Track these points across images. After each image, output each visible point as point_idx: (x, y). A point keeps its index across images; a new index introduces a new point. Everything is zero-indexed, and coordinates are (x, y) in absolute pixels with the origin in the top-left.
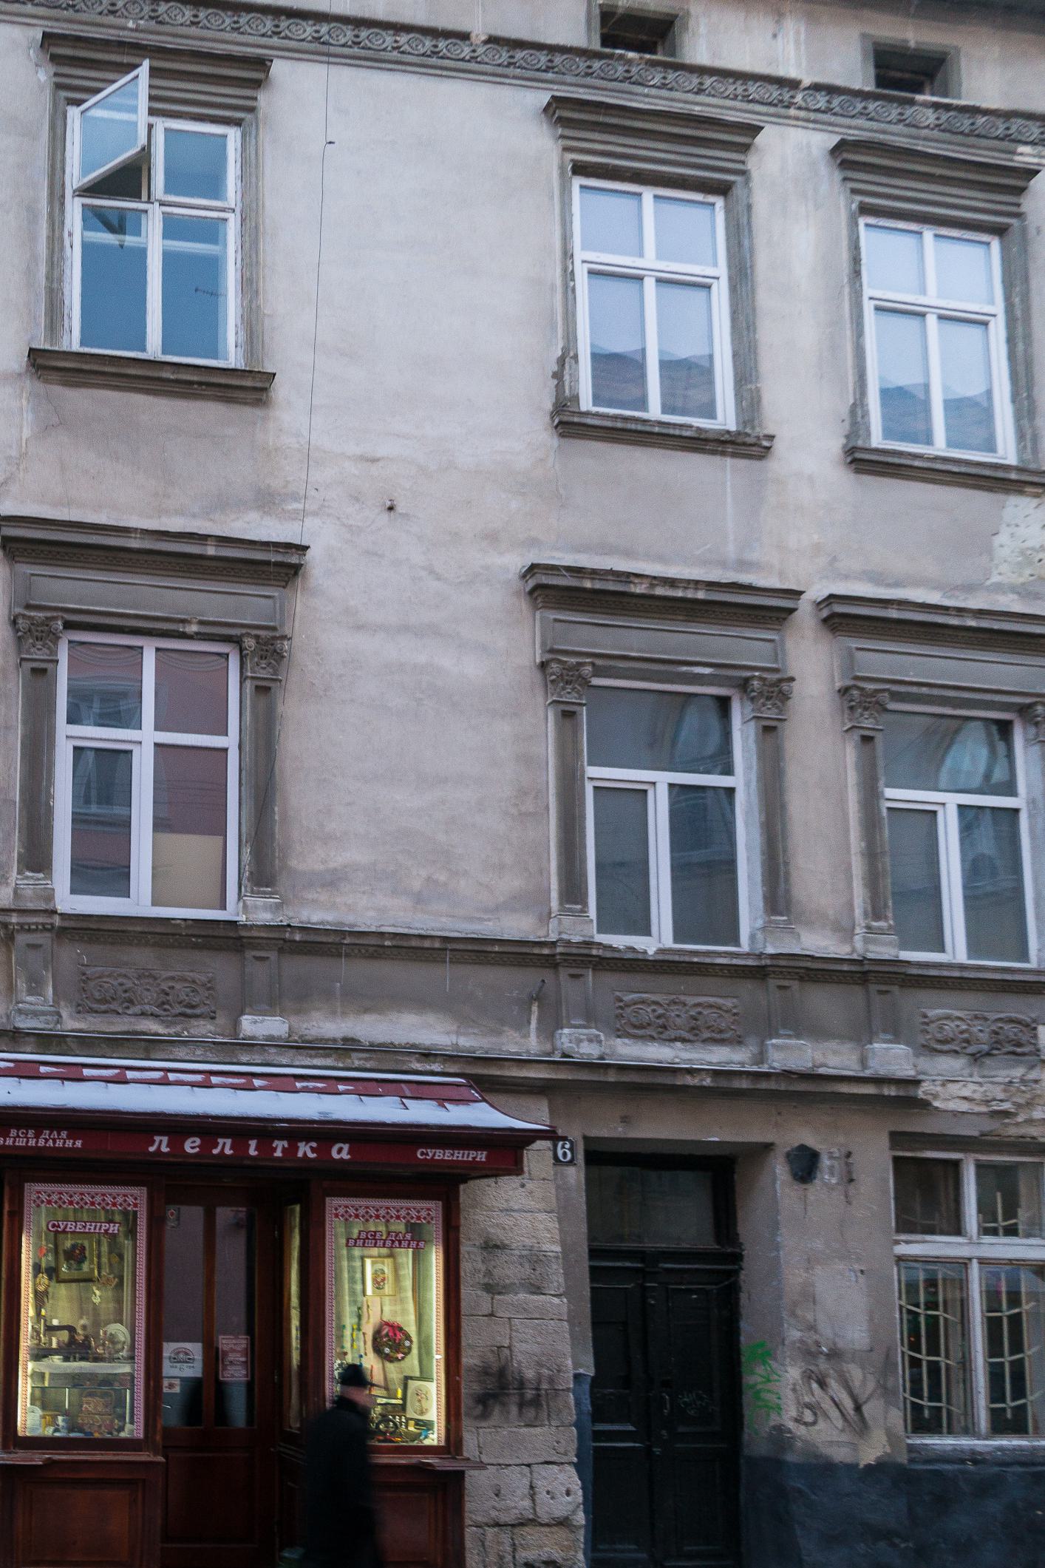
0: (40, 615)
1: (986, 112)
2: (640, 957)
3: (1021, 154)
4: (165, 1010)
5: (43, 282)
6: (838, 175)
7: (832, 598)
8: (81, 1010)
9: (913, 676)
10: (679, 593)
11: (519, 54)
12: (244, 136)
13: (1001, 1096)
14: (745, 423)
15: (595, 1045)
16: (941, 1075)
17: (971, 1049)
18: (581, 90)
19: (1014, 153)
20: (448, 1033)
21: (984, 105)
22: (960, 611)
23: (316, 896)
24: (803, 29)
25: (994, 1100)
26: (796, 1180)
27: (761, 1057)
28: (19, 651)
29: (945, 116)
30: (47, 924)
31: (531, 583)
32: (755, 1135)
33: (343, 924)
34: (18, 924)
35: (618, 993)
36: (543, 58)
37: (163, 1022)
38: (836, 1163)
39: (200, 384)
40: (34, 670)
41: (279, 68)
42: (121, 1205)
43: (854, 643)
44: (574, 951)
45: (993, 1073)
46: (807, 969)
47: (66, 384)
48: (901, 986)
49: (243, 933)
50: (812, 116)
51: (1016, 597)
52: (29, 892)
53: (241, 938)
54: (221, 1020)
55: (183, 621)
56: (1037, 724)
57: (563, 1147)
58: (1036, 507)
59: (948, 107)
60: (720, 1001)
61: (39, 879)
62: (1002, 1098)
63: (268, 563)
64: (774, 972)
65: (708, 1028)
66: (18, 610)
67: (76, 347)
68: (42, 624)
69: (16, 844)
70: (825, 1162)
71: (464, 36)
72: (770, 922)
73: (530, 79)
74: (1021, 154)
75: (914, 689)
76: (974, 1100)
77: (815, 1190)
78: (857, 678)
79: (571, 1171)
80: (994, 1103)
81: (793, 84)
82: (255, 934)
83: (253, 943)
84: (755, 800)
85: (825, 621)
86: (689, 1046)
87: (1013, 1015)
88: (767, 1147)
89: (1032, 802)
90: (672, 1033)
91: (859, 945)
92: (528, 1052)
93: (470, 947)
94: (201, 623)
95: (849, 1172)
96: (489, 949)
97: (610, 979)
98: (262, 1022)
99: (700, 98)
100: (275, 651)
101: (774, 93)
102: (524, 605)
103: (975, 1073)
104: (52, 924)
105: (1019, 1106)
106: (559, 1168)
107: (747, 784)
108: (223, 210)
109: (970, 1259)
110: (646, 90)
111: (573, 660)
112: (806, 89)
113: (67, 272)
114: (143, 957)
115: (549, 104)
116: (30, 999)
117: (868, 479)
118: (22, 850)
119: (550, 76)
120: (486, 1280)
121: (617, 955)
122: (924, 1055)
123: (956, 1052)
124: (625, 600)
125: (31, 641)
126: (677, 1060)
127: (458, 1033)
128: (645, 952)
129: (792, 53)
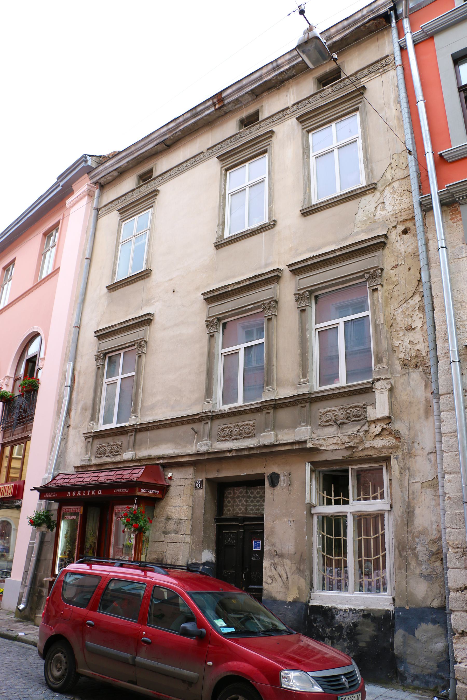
2: (223, 412)
3: (363, 81)
9: (320, 281)
13: (348, 440)
15: (206, 446)
16: (326, 436)
19: (361, 82)
20: (173, 449)
25: (345, 442)
32: (258, 471)
33: (154, 420)
35: (219, 427)
41: (158, 189)
44: (204, 415)
45: (347, 431)
49: (126, 429)
51: (364, 234)
55: (126, 344)
57: (198, 483)
62: (348, 441)
64: (264, 408)
65: (245, 433)
70: (282, 478)
74: (363, 81)
75: (321, 286)
76: (339, 444)
79: (201, 491)
80: (345, 444)
86: (238, 441)
90: (233, 438)
103: (339, 433)
105: (357, 443)
106: (197, 490)
109: (348, 512)
114: (109, 440)
120: (164, 530)
121: (217, 413)
122: (319, 429)
124: (228, 293)
126: (234, 447)
127: (175, 449)
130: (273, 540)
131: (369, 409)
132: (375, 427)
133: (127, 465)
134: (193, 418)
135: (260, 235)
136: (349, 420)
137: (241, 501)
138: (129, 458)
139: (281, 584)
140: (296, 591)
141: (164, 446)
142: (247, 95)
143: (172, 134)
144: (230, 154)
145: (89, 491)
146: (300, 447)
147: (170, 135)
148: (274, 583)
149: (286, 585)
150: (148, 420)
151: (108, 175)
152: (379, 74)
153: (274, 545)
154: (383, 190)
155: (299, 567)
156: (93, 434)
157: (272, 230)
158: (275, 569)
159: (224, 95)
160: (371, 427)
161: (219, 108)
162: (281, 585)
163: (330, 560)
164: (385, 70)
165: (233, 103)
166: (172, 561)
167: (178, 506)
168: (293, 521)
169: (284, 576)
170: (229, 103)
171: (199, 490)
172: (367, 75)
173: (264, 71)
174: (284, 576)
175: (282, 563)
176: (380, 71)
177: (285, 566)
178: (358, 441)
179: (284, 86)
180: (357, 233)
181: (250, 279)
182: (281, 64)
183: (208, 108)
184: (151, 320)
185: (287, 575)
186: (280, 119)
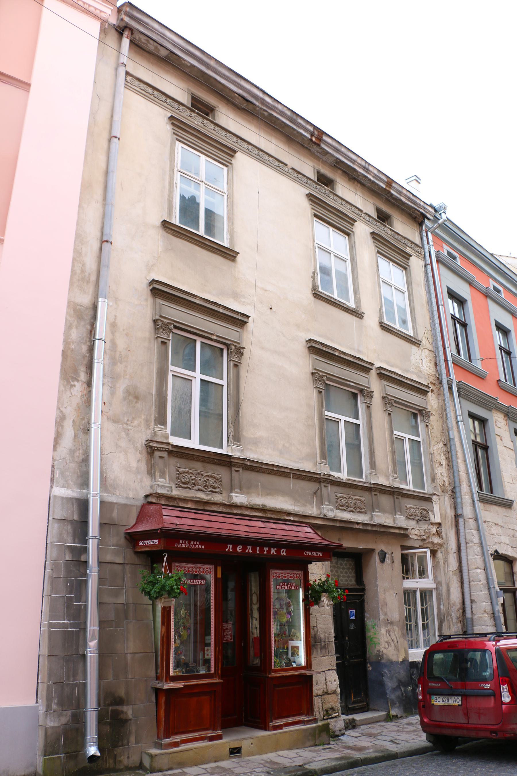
0: (166, 321)
1: (400, 235)
4: (206, 489)
5: (167, 197)
6: (372, 240)
7: (380, 368)
8: (178, 486)
10: (346, 358)
11: (300, 176)
12: (228, 171)
14: (357, 307)
15: (332, 512)
17: (417, 518)
21: (400, 233)
22: (407, 378)
23: (251, 447)
27: (372, 518)
28: (155, 333)
29: (393, 233)
31: (309, 345)
32: (370, 546)
33: (259, 459)
34: (156, 447)
35: (336, 493)
36: (305, 180)
37: (205, 494)
40: (162, 342)
42: (191, 571)
43: (386, 383)
46: (381, 489)
48: (401, 497)
49: (232, 460)
50: (366, 221)
52: (159, 433)
53: (231, 462)
54: (224, 495)
55: (212, 334)
56: (423, 416)
59: (393, 231)
60: (361, 498)
61: (162, 429)
63: (238, 319)
65: (358, 507)
66: (157, 317)
67: (177, 223)
68: (166, 325)
69: (153, 412)
71: (286, 165)
72: (371, 472)
78: (386, 394)
81: (362, 211)
82: (236, 461)
83: (236, 465)
84: (366, 430)
85: (378, 374)
87: (424, 508)
88: (373, 550)
89: (423, 440)
90: (350, 509)
91: (391, 482)
92: (314, 513)
93: (297, 473)
94: (217, 336)
95: (393, 559)
96: (303, 474)
97: (335, 489)
98: (239, 496)
99: (341, 206)
100: (240, 352)
101: (358, 212)
102: (306, 351)
104: (168, 449)
107: (363, 424)
108: (223, 193)
110: (330, 199)
111: (321, 374)
113: (174, 196)
114: (198, 466)
115: (308, 194)
116: (160, 480)
117: (384, 331)
118: (157, 416)
119: (307, 185)
123: (413, 519)
124: (333, 356)
125: (161, 330)
128: (343, 480)
131: (430, 513)
133: (247, 513)
134: (313, 476)
138: (242, 503)
139: (394, 647)
141: (280, 498)
144: (321, 203)
145: (266, 549)
146: (404, 533)
147: (260, 106)
149: (397, 649)
150: (251, 456)
151: (155, 44)
153: (386, 614)
156: (170, 448)
159: (324, 138)
161: (314, 143)
164: (418, 256)
169: (396, 641)
176: (417, 253)
178: (427, 536)
179: (354, 183)
180: (412, 373)
181: (354, 357)
182: (370, 171)
183: (306, 130)
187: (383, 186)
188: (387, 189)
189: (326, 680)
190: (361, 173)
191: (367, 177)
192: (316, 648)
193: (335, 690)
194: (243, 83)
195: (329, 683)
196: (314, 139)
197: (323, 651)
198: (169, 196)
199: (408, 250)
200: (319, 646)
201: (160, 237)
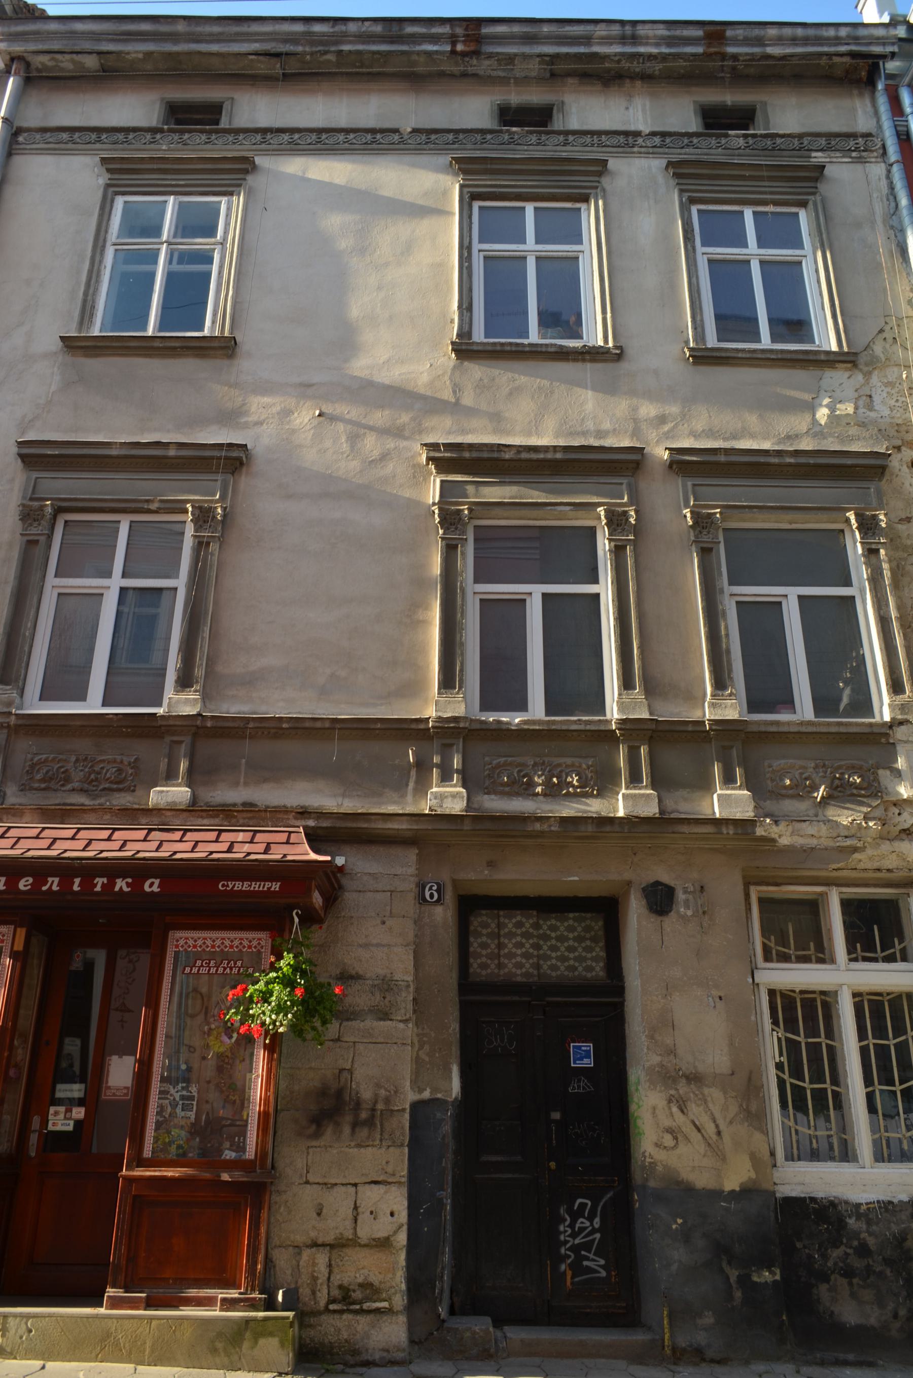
3: (815, 157)
6: (673, 182)
18: (478, 152)
19: (810, 157)
20: (335, 796)
24: (648, 103)
26: (653, 912)
30: (5, 723)
35: (487, 759)
38: (691, 897)
39: (182, 348)
47: (86, 356)
55: (147, 501)
57: (431, 888)
58: (849, 378)
61: (7, 690)
70: (681, 896)
71: (396, 131)
73: (441, 150)
74: (815, 157)
77: (670, 922)
79: (439, 910)
80: (839, 839)
81: (637, 134)
93: (355, 726)
96: (372, 726)
99: (568, 148)
104: (8, 723)
112: (646, 135)
114: (84, 745)
127: (344, 796)
129: (640, 118)
130: (669, 1041)
132: (899, 814)
135: (579, 365)
136: (840, 792)
137: (520, 945)
139: (702, 1148)
140: (748, 1164)
142: (538, 59)
143: (314, 49)
145: (100, 882)
147: (307, 49)
148: (681, 1145)
149: (715, 1149)
151: (68, 57)
152: (850, 160)
154: (870, 373)
155: (747, 1106)
157: (610, 366)
158: (682, 1112)
159: (486, 30)
160: (890, 814)
161: (464, 54)
162: (702, 1151)
163: (798, 1092)
165: (498, 60)
166: (376, 1095)
167: (378, 945)
168: (720, 998)
169: (710, 1129)
170: (490, 56)
171: (433, 907)
172: (825, 150)
173: (601, 31)
174: (710, 1129)
175: (700, 1096)
176: (854, 154)
177: (710, 1105)
183: (434, 39)
184: (242, 464)
185: (717, 1126)
186: (619, 147)
187: (700, 50)
188: (712, 50)
189: (356, 1208)
190: (616, 54)
191: (640, 55)
192: (337, 1124)
193: (387, 1239)
194: (255, 28)
195: (364, 1217)
196: (460, 47)
197: (364, 1132)
198: (86, 294)
199: (818, 157)
200: (349, 1118)
201: (56, 369)
